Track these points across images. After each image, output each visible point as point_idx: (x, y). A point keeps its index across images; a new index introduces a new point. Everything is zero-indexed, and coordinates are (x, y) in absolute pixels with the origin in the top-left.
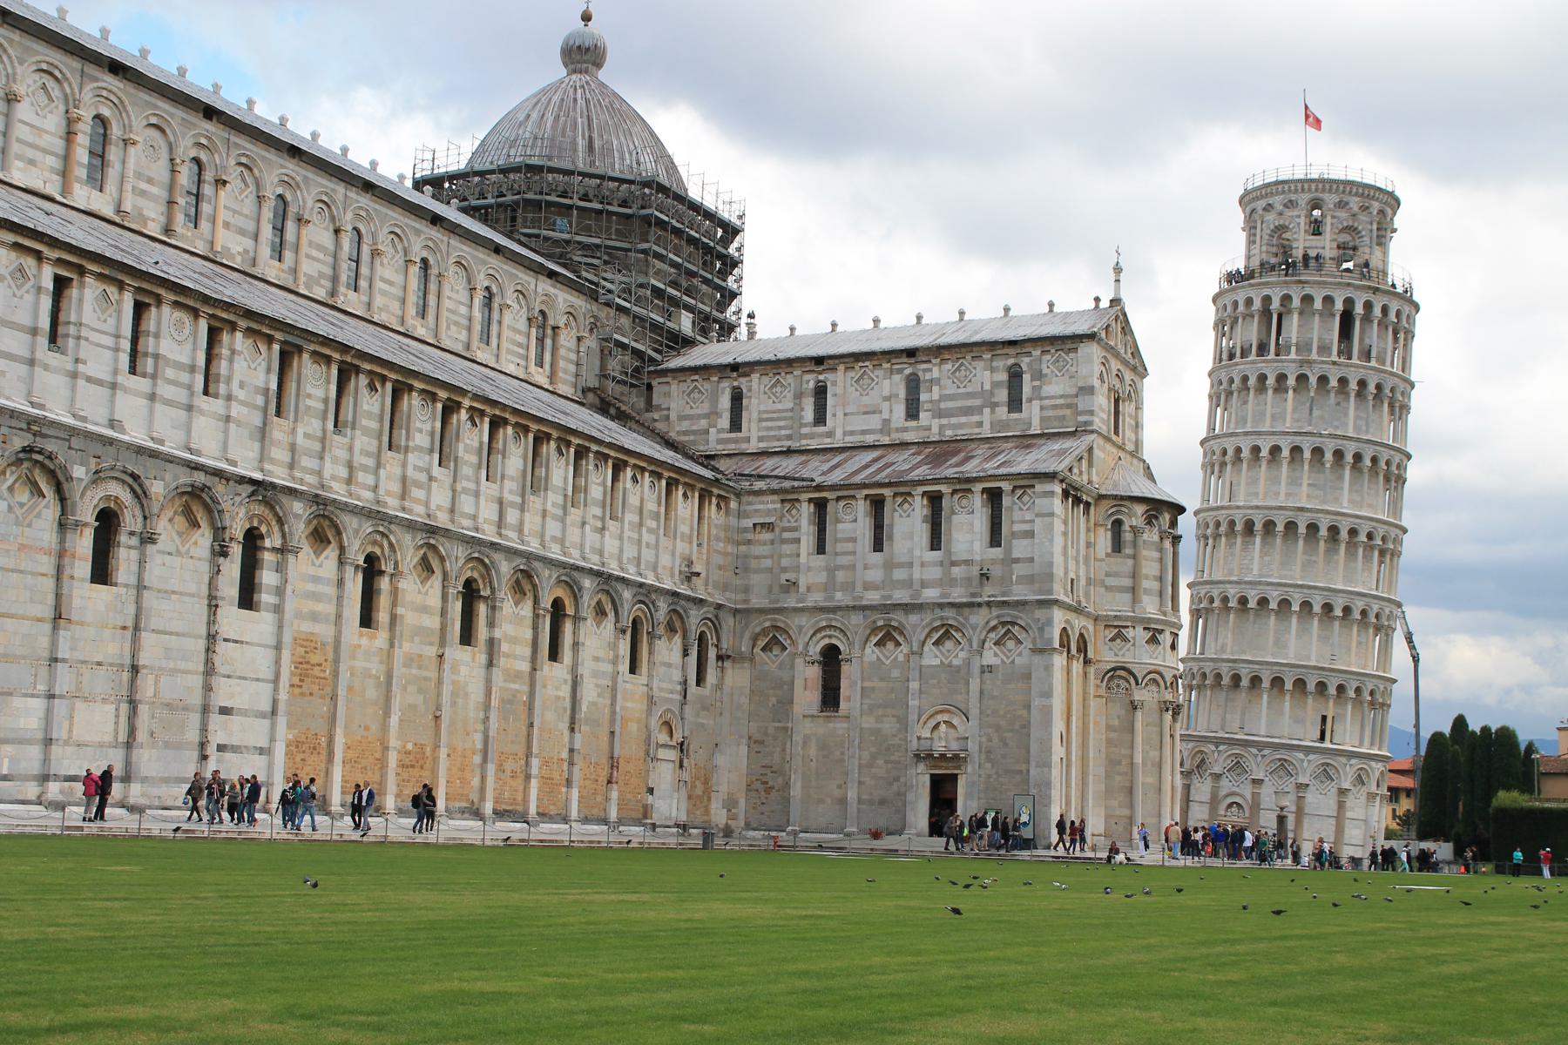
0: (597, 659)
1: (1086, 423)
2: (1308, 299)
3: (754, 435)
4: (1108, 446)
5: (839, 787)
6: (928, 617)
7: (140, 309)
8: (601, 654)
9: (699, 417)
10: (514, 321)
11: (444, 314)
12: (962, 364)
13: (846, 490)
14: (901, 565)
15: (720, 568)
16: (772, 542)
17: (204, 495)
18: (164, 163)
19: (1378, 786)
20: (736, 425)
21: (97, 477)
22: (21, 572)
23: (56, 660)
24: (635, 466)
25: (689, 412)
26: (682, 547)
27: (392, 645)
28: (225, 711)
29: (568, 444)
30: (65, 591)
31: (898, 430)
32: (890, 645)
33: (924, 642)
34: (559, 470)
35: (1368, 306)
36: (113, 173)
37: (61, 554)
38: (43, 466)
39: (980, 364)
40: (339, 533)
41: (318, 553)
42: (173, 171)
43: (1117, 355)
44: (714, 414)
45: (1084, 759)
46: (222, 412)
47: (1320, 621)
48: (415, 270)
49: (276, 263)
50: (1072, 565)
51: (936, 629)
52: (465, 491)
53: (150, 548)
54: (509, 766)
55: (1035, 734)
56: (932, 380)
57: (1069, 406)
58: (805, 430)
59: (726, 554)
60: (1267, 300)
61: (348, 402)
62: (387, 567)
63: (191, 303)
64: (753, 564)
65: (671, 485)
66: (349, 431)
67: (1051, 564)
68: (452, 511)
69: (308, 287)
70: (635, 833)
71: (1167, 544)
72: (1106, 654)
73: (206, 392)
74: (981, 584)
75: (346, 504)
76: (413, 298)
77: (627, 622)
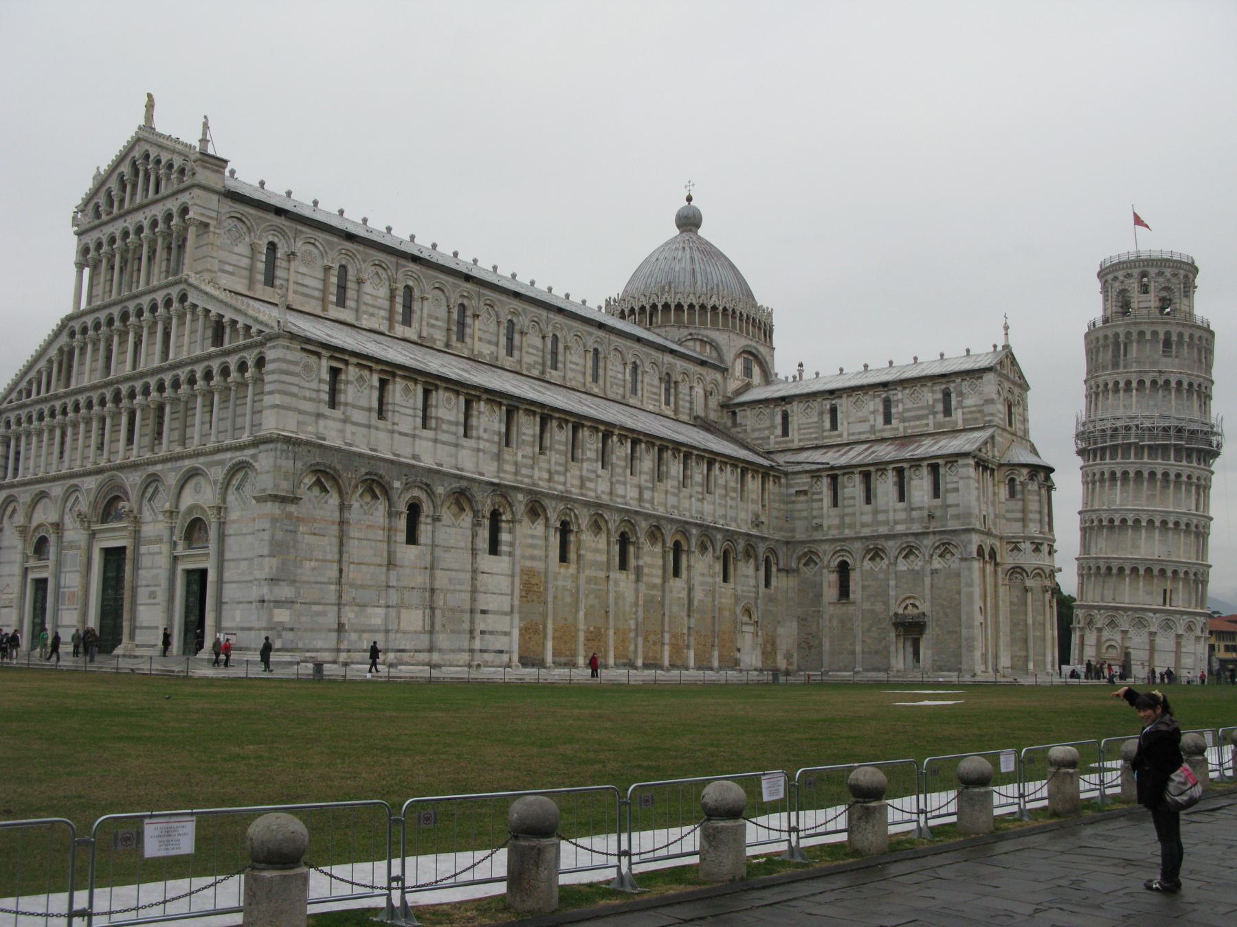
0: (703, 575)
1: (990, 421)
2: (1141, 334)
4: (1005, 434)
5: (851, 644)
7: (427, 393)
8: (705, 571)
10: (650, 381)
11: (608, 379)
13: (848, 469)
15: (777, 518)
16: (807, 501)
17: (467, 493)
18: (444, 308)
19: (1202, 631)
20: (785, 433)
21: (407, 487)
22: (367, 540)
23: (389, 587)
24: (721, 461)
25: (758, 426)
26: (751, 507)
27: (579, 572)
28: (484, 612)
29: (679, 451)
30: (392, 549)
31: (880, 431)
32: (878, 560)
33: (897, 558)
34: (675, 468)
35: (1180, 335)
38: (379, 484)
39: (925, 389)
40: (545, 510)
41: (533, 523)
42: (449, 312)
43: (1008, 379)
44: (773, 427)
45: (996, 623)
46: (475, 446)
47: (1161, 531)
48: (590, 355)
49: (511, 359)
50: (983, 507)
51: (904, 549)
52: (618, 482)
53: (438, 524)
54: (651, 638)
55: (964, 609)
56: (898, 401)
57: (980, 411)
58: (826, 434)
59: (780, 510)
60: (1117, 335)
61: (547, 435)
62: (575, 528)
63: (455, 388)
64: (797, 514)
65: (744, 472)
66: (548, 452)
69: (529, 370)
70: (732, 675)
71: (1043, 491)
72: (1008, 559)
73: (466, 436)
74: (929, 521)
75: (548, 494)
76: (589, 372)
77: (719, 553)
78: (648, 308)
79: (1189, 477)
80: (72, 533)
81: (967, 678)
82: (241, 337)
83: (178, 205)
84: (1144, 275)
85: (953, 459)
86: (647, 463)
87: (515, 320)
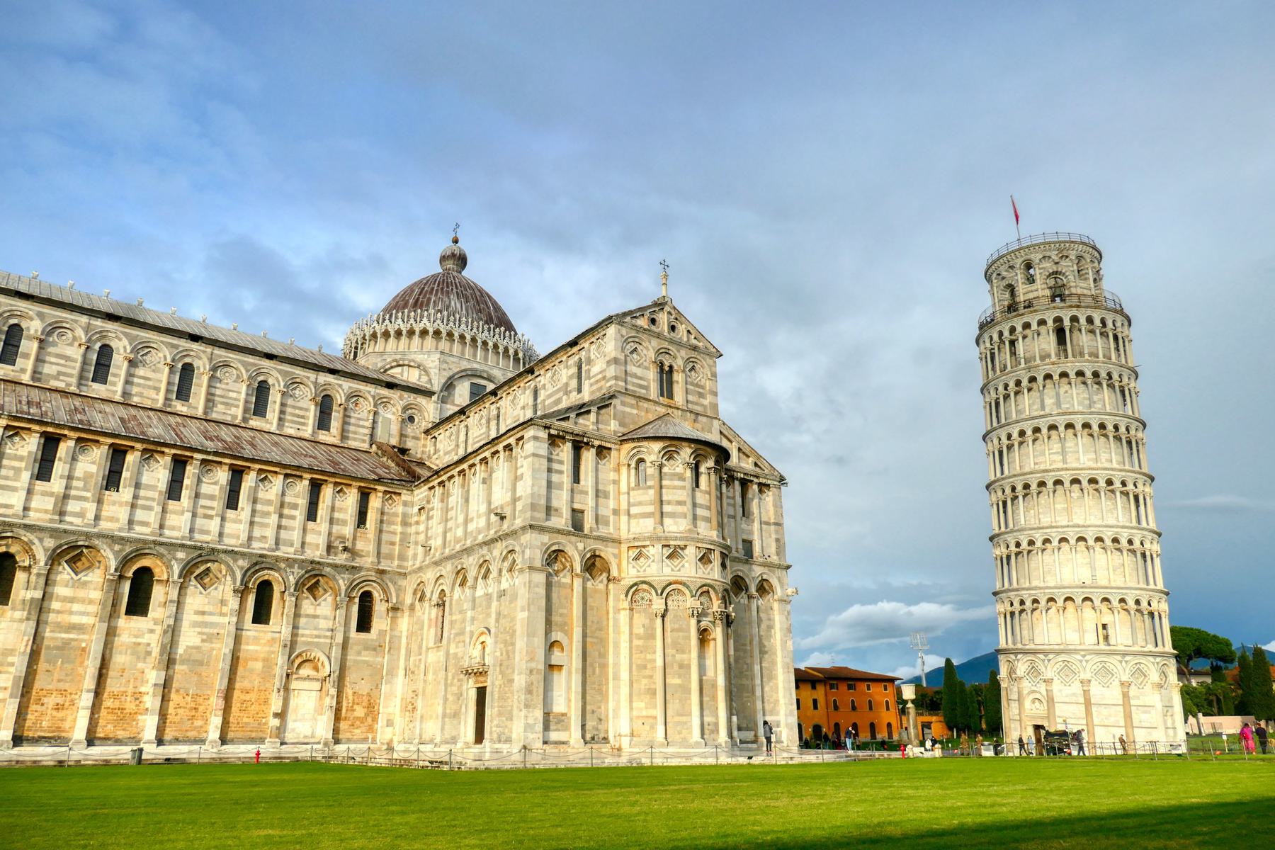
4: (646, 405)
6: (476, 556)
8: (206, 609)
12: (556, 371)
24: (260, 470)
33: (476, 579)
35: (1074, 319)
39: (562, 366)
43: (659, 336)
44: (457, 446)
51: (481, 566)
54: (50, 701)
60: (1001, 334)
71: (688, 473)
72: (629, 572)
79: (1109, 482)
84: (1029, 266)
87: (24, 325)
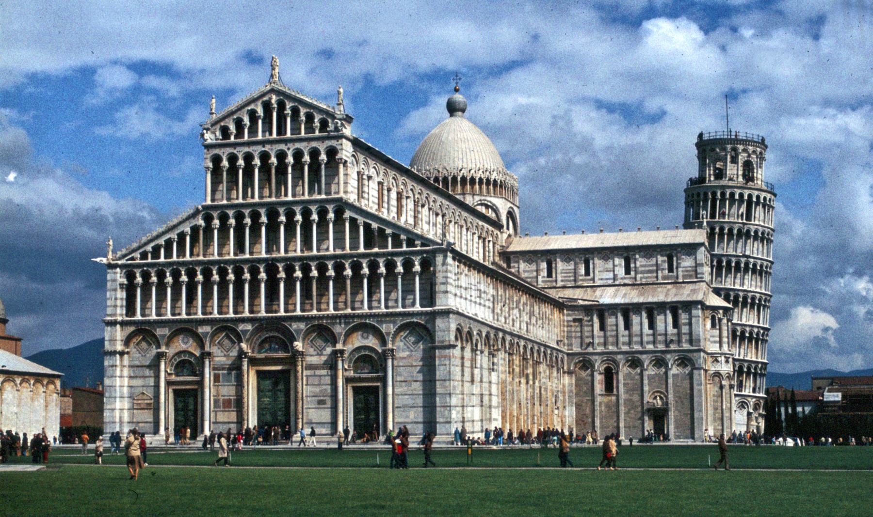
1: (702, 278)
3: (559, 278)
6: (651, 355)
9: (532, 271)
14: (636, 335)
25: (527, 269)
31: (622, 279)
34: (536, 308)
35: (758, 197)
36: (404, 209)
37: (472, 361)
40: (505, 342)
42: (415, 205)
57: (693, 271)
58: (581, 278)
64: (573, 334)
67: (699, 335)
68: (520, 328)
72: (712, 368)
78: (450, 178)
80: (224, 359)
81: (698, 443)
82: (404, 245)
83: (325, 146)
85: (688, 306)
86: (528, 307)
